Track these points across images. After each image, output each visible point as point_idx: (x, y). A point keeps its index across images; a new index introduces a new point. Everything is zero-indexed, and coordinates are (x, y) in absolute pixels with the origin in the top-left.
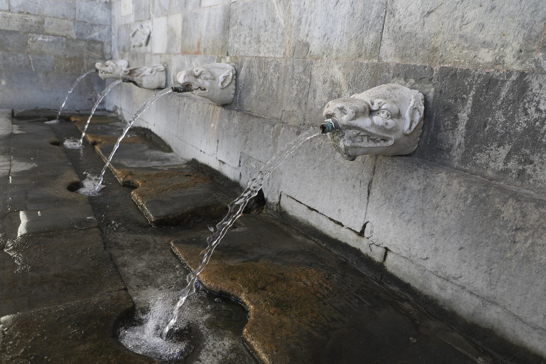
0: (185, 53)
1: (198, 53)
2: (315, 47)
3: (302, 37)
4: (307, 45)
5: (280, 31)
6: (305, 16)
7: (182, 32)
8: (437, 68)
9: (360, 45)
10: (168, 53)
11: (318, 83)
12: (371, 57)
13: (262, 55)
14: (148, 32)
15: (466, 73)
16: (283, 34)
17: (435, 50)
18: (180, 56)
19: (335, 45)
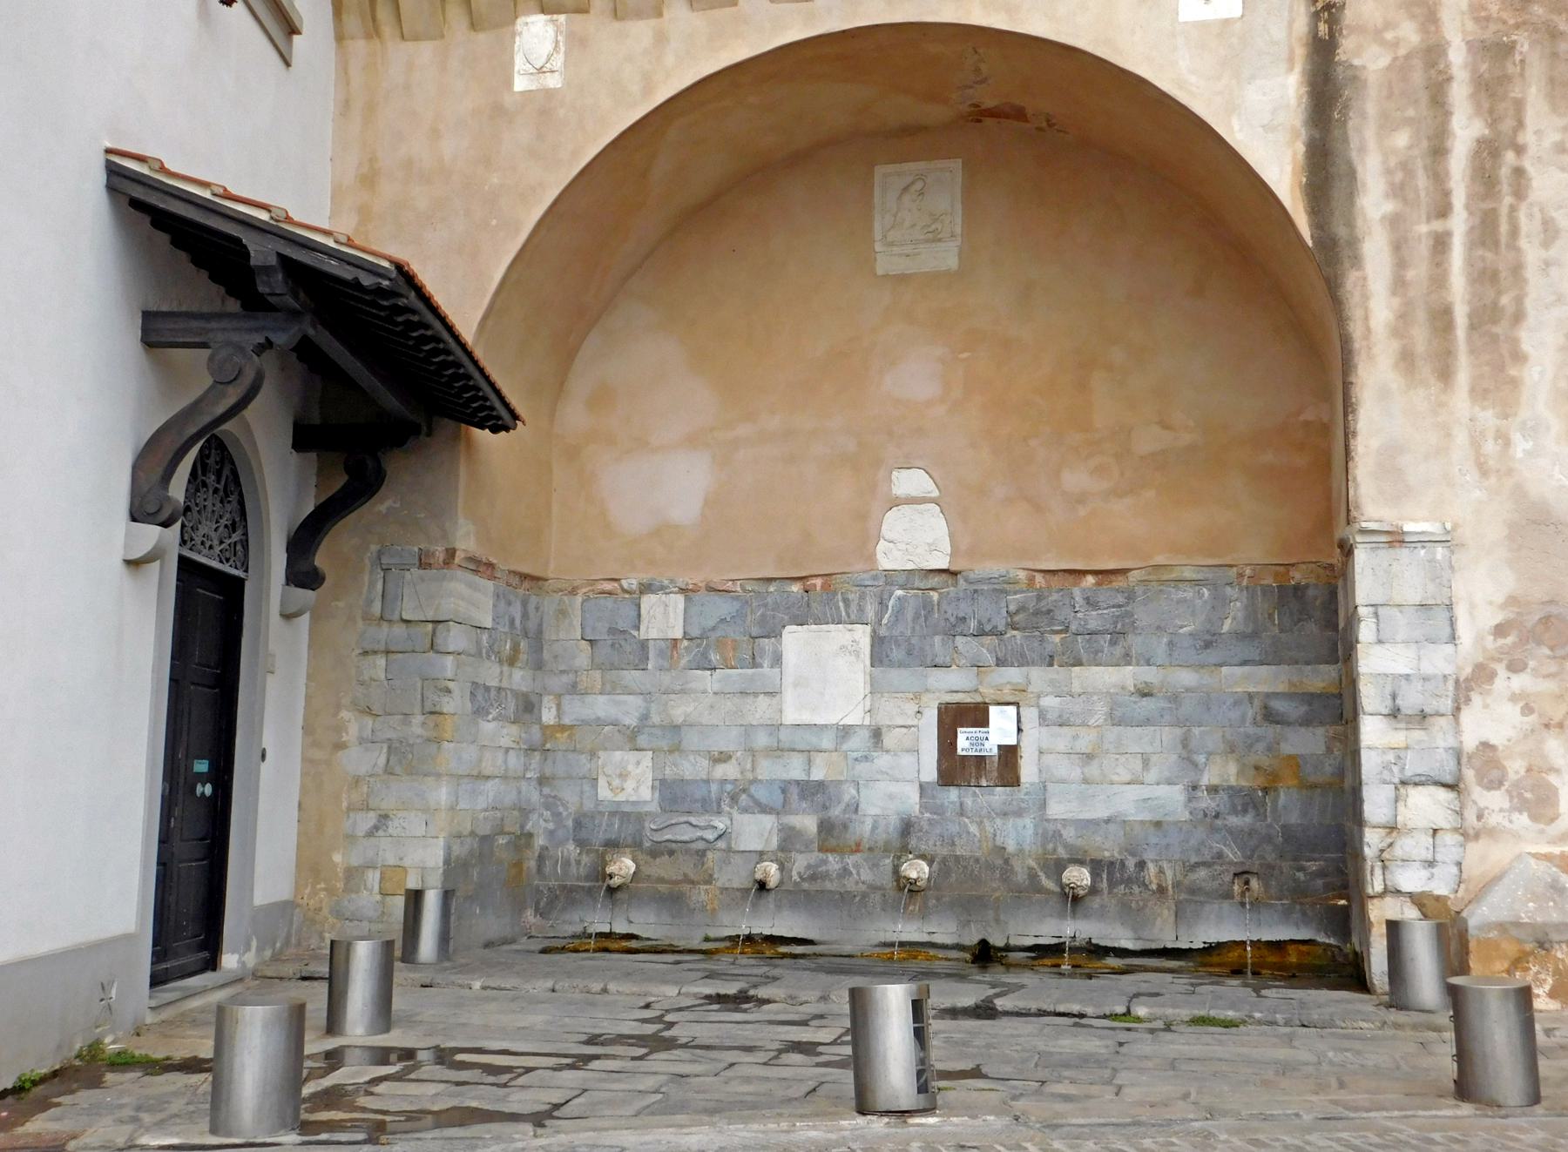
0: (827, 851)
1: (857, 851)
2: (1011, 847)
3: (999, 841)
4: (1004, 848)
5: (976, 840)
6: (999, 832)
7: (820, 832)
8: (1088, 859)
9: (1045, 849)
10: (782, 848)
11: (1018, 868)
12: (1053, 854)
13: (958, 853)
14: (721, 826)
15: (1101, 861)
16: (980, 841)
17: (1086, 852)
18: (816, 853)
19: (1027, 848)
